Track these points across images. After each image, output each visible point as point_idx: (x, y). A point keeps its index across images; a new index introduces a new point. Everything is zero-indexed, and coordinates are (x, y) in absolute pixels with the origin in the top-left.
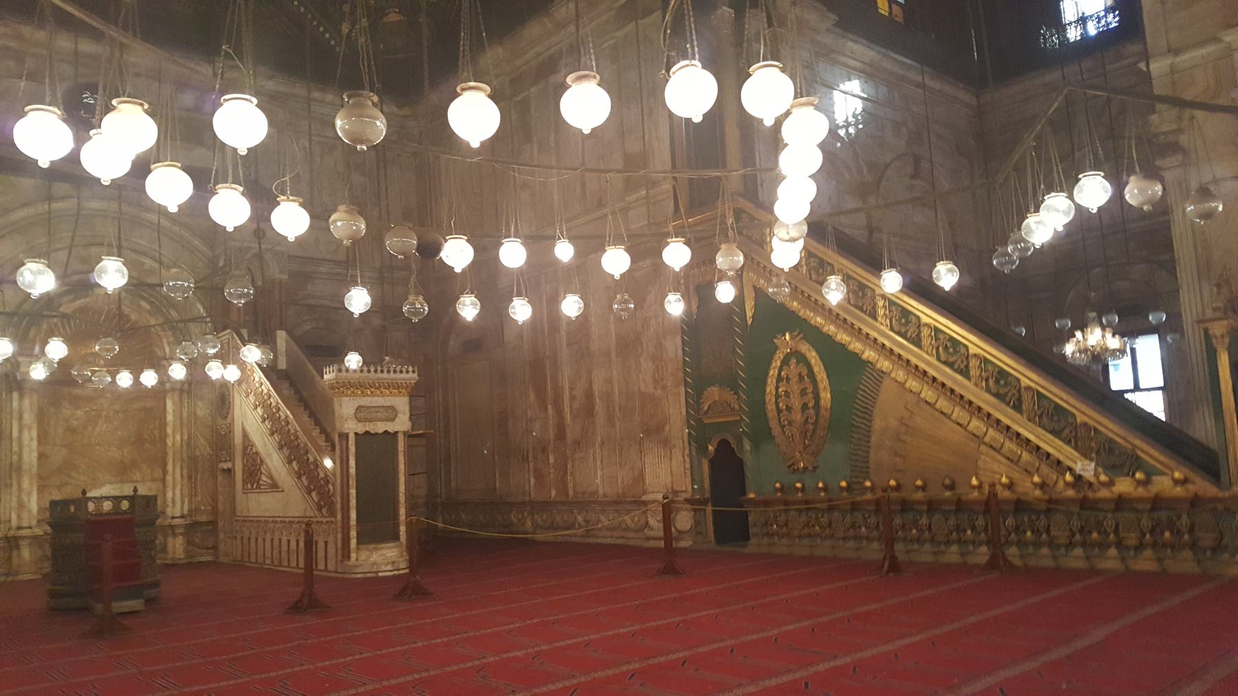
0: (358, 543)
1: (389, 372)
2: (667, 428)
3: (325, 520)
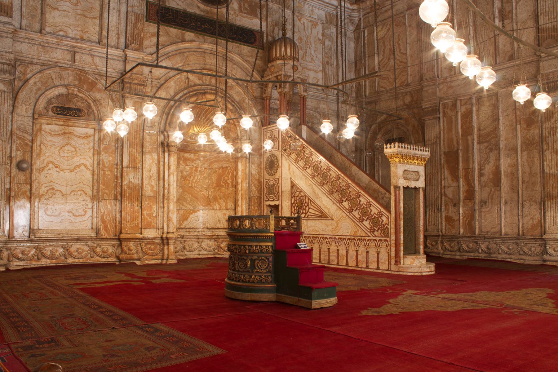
3: (378, 239)
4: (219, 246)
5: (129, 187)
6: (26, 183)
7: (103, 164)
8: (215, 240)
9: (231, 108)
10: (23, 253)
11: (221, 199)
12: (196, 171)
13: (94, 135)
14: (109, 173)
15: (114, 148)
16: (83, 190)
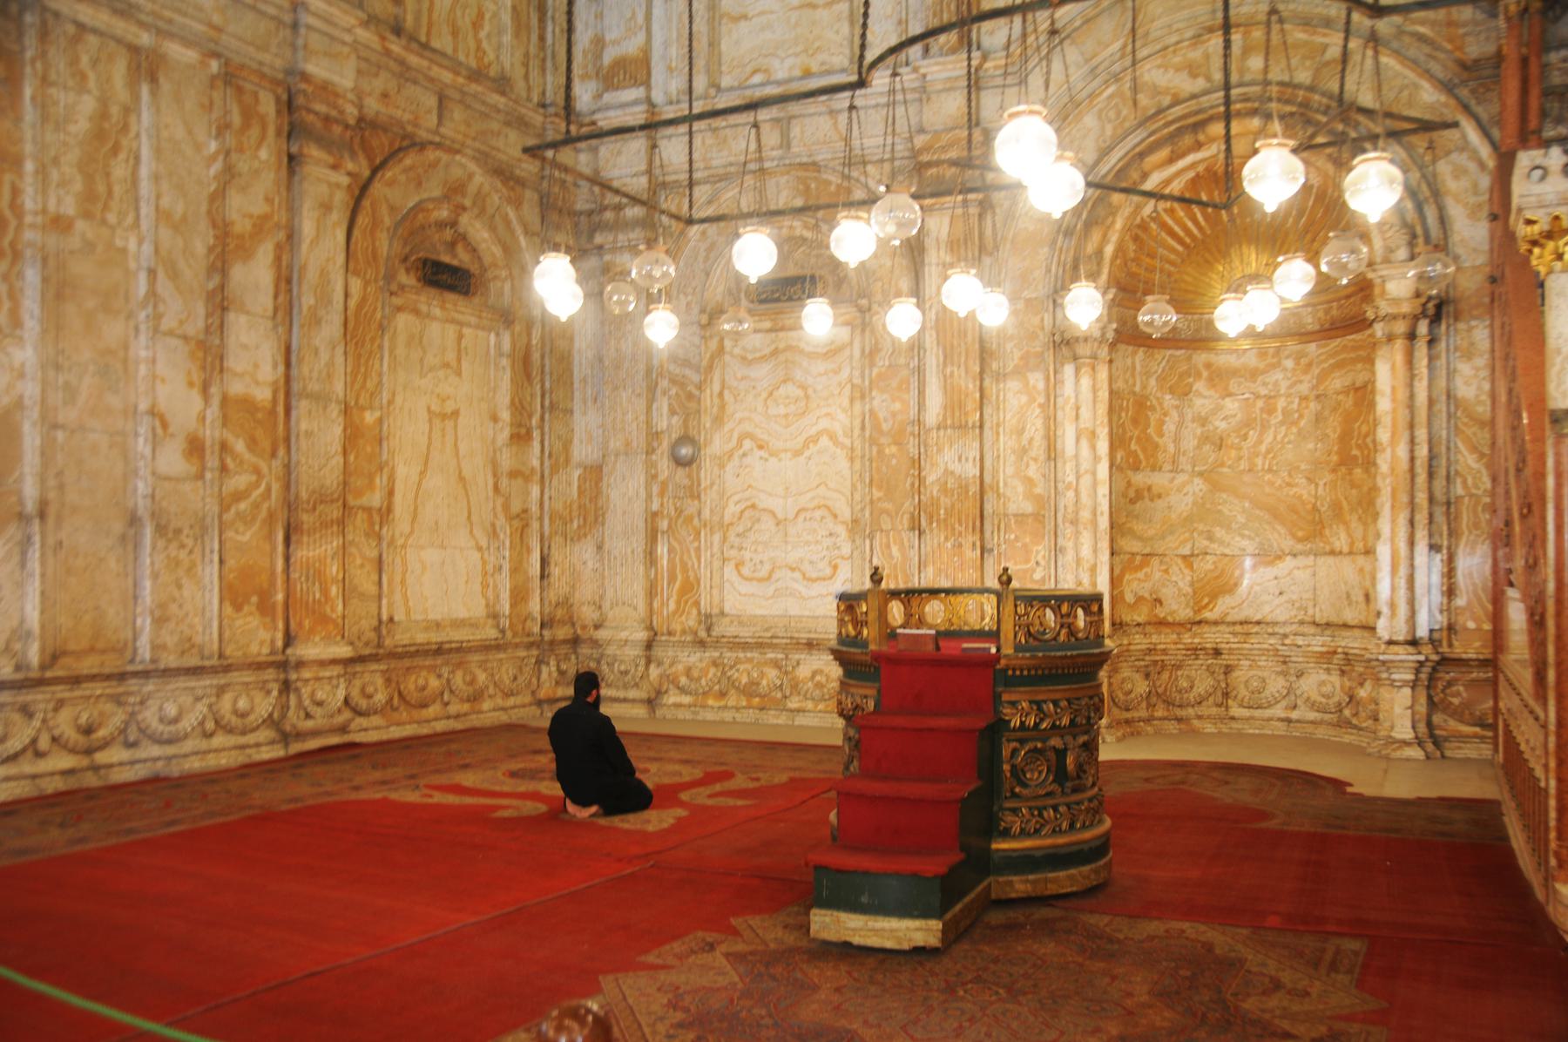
5: (944, 490)
6: (692, 497)
7: (877, 426)
8: (1343, 672)
11: (1352, 510)
12: (1270, 411)
13: (851, 343)
14: (894, 449)
15: (905, 373)
16: (828, 508)
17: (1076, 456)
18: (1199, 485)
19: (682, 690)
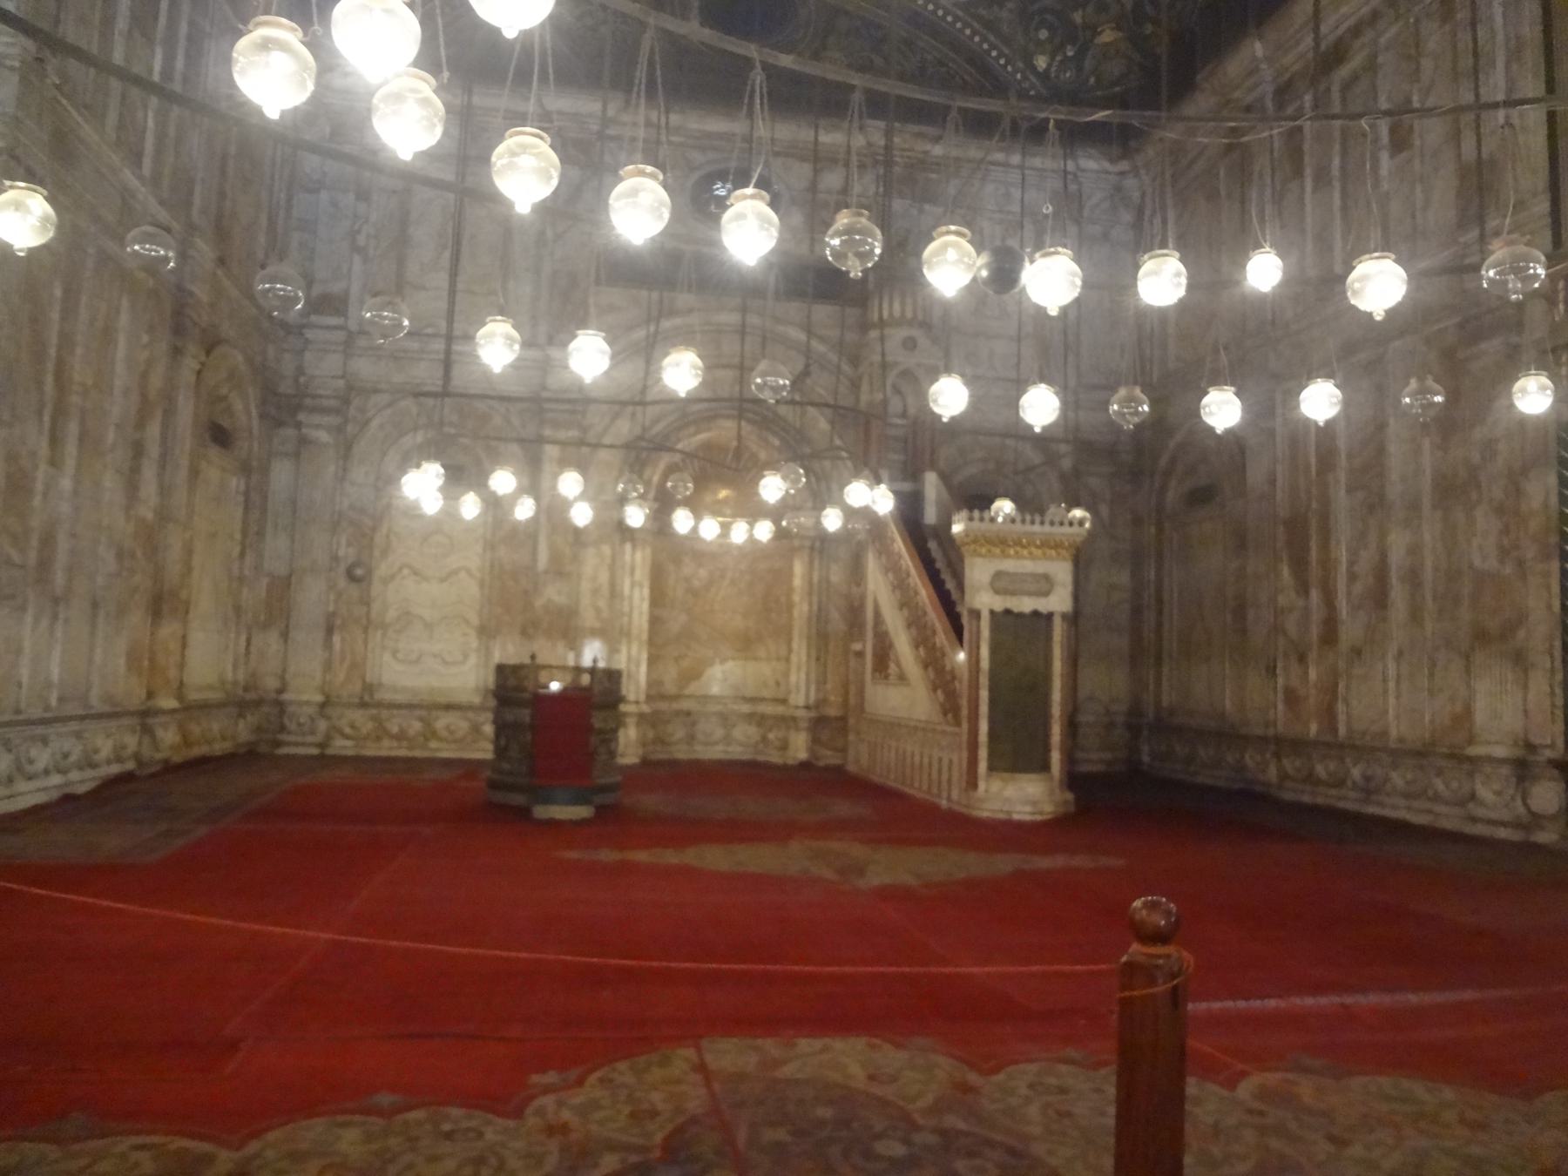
0: (992, 768)
1: (1042, 523)
2: (1521, 634)
4: (764, 739)
9: (777, 442)
10: (353, 727)
17: (631, 598)
18: (683, 618)
19: (347, 737)
